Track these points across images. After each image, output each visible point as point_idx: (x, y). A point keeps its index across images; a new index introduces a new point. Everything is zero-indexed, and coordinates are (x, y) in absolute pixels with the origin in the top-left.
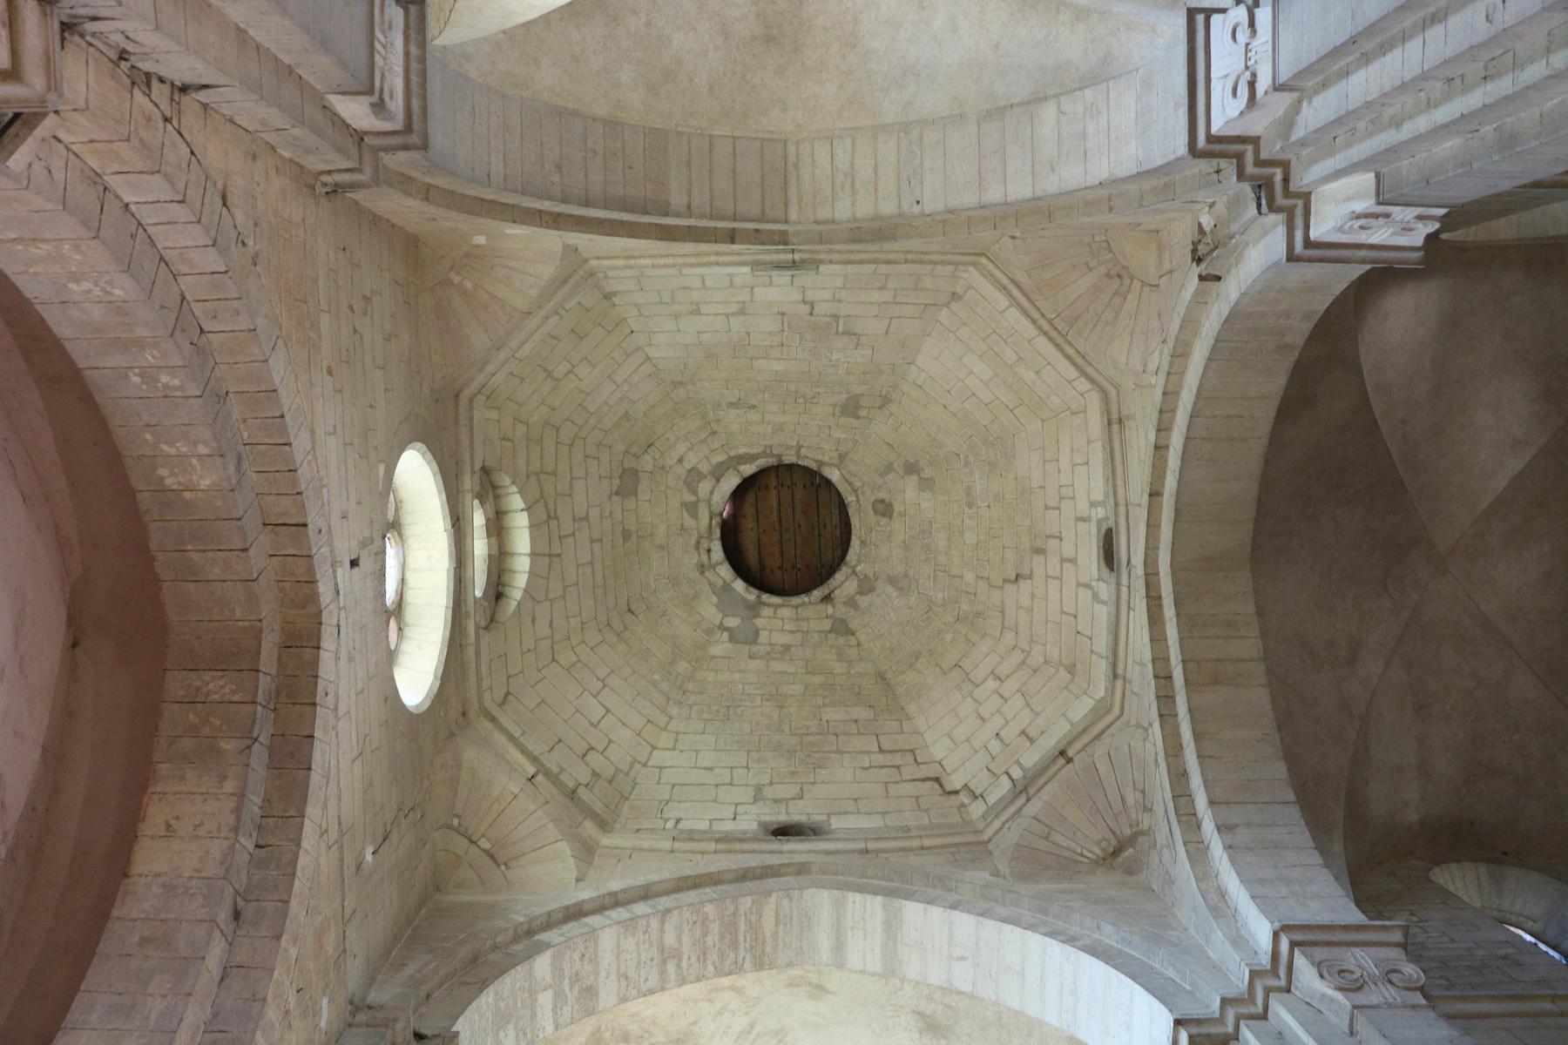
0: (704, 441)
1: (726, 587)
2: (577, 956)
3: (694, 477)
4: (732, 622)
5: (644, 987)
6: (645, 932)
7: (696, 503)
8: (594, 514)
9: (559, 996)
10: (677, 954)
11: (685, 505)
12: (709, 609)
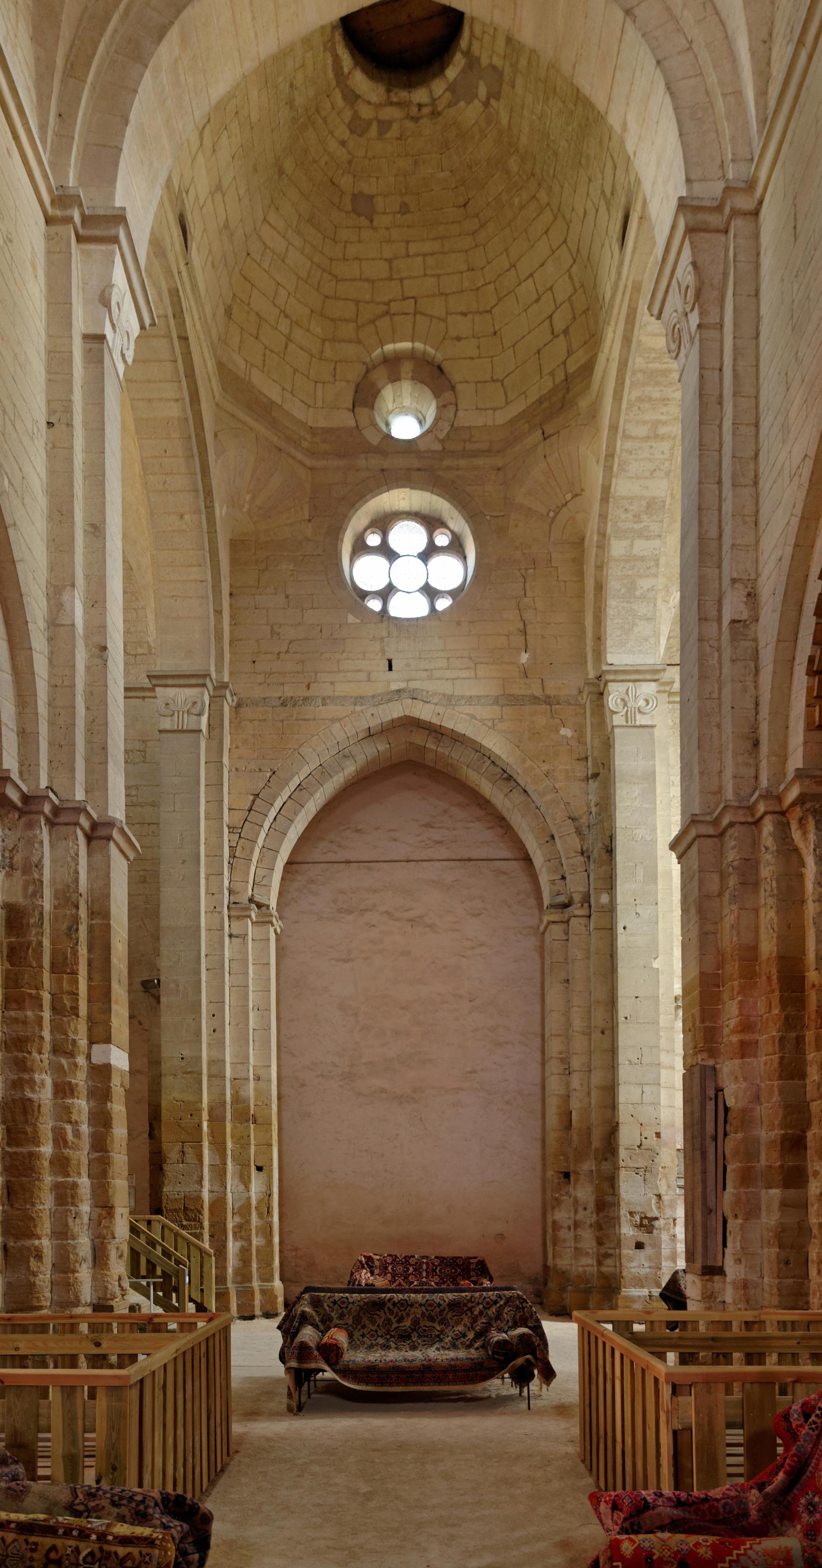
0: (325, 119)
1: (452, 88)
2: (623, 516)
3: (357, 127)
4: (482, 91)
5: (667, 455)
6: (631, 453)
7: (380, 122)
8: (387, 253)
9: (642, 534)
10: (657, 423)
11: (381, 134)
12: (470, 113)
